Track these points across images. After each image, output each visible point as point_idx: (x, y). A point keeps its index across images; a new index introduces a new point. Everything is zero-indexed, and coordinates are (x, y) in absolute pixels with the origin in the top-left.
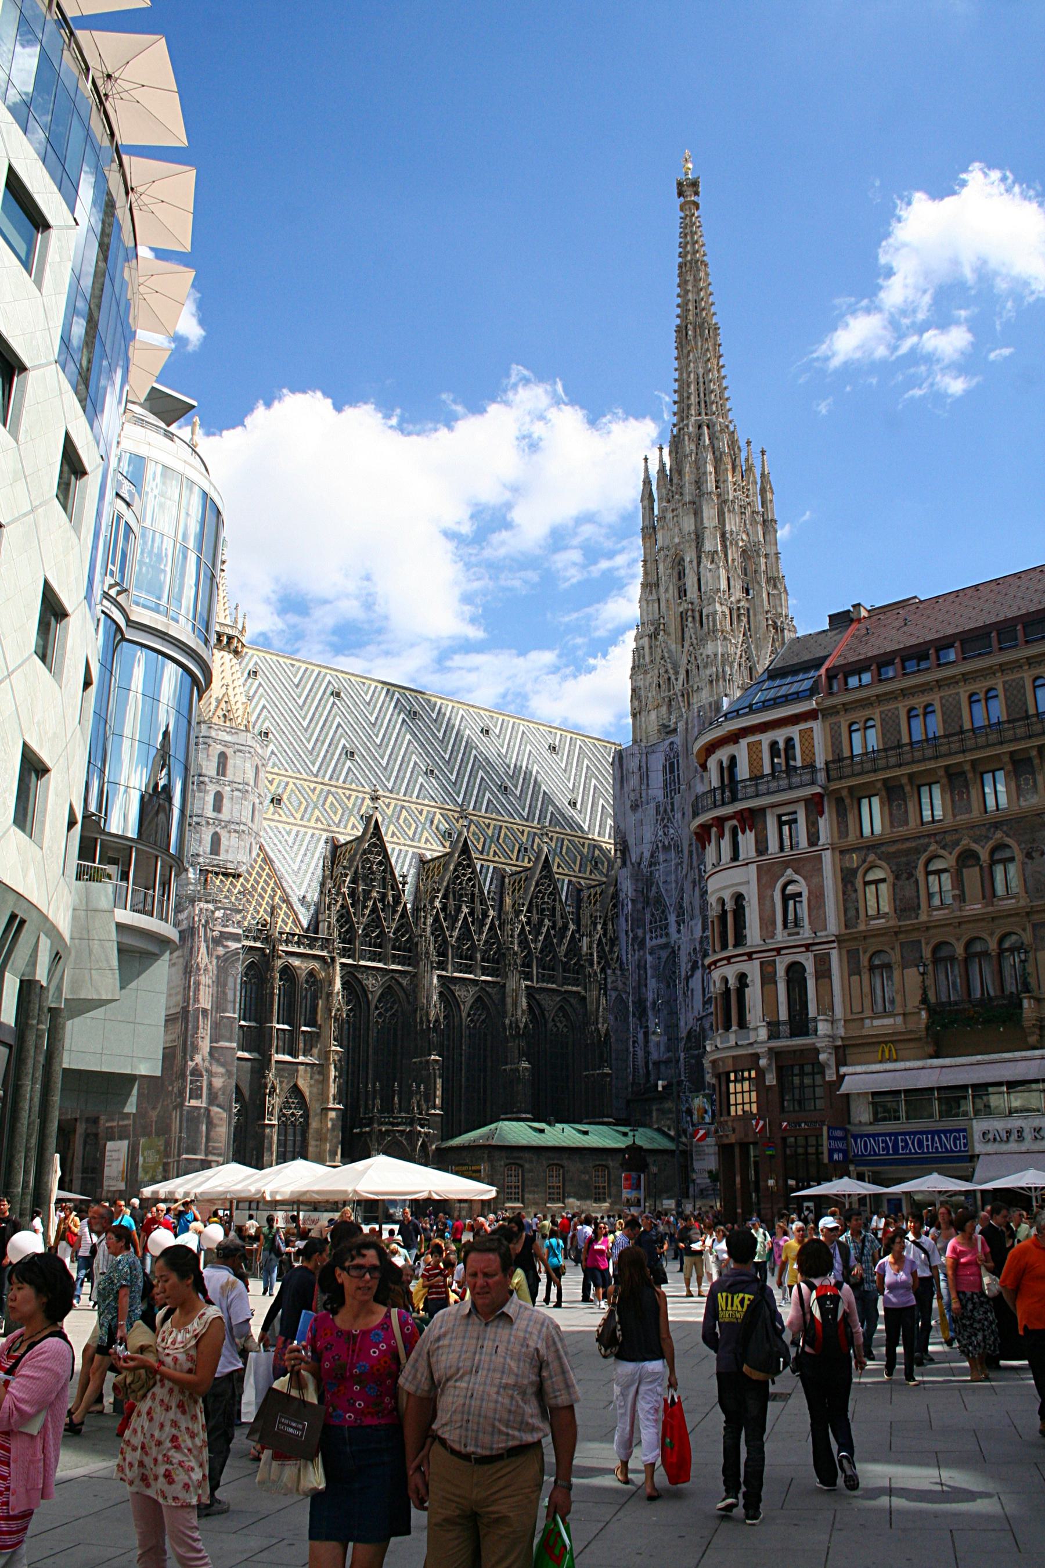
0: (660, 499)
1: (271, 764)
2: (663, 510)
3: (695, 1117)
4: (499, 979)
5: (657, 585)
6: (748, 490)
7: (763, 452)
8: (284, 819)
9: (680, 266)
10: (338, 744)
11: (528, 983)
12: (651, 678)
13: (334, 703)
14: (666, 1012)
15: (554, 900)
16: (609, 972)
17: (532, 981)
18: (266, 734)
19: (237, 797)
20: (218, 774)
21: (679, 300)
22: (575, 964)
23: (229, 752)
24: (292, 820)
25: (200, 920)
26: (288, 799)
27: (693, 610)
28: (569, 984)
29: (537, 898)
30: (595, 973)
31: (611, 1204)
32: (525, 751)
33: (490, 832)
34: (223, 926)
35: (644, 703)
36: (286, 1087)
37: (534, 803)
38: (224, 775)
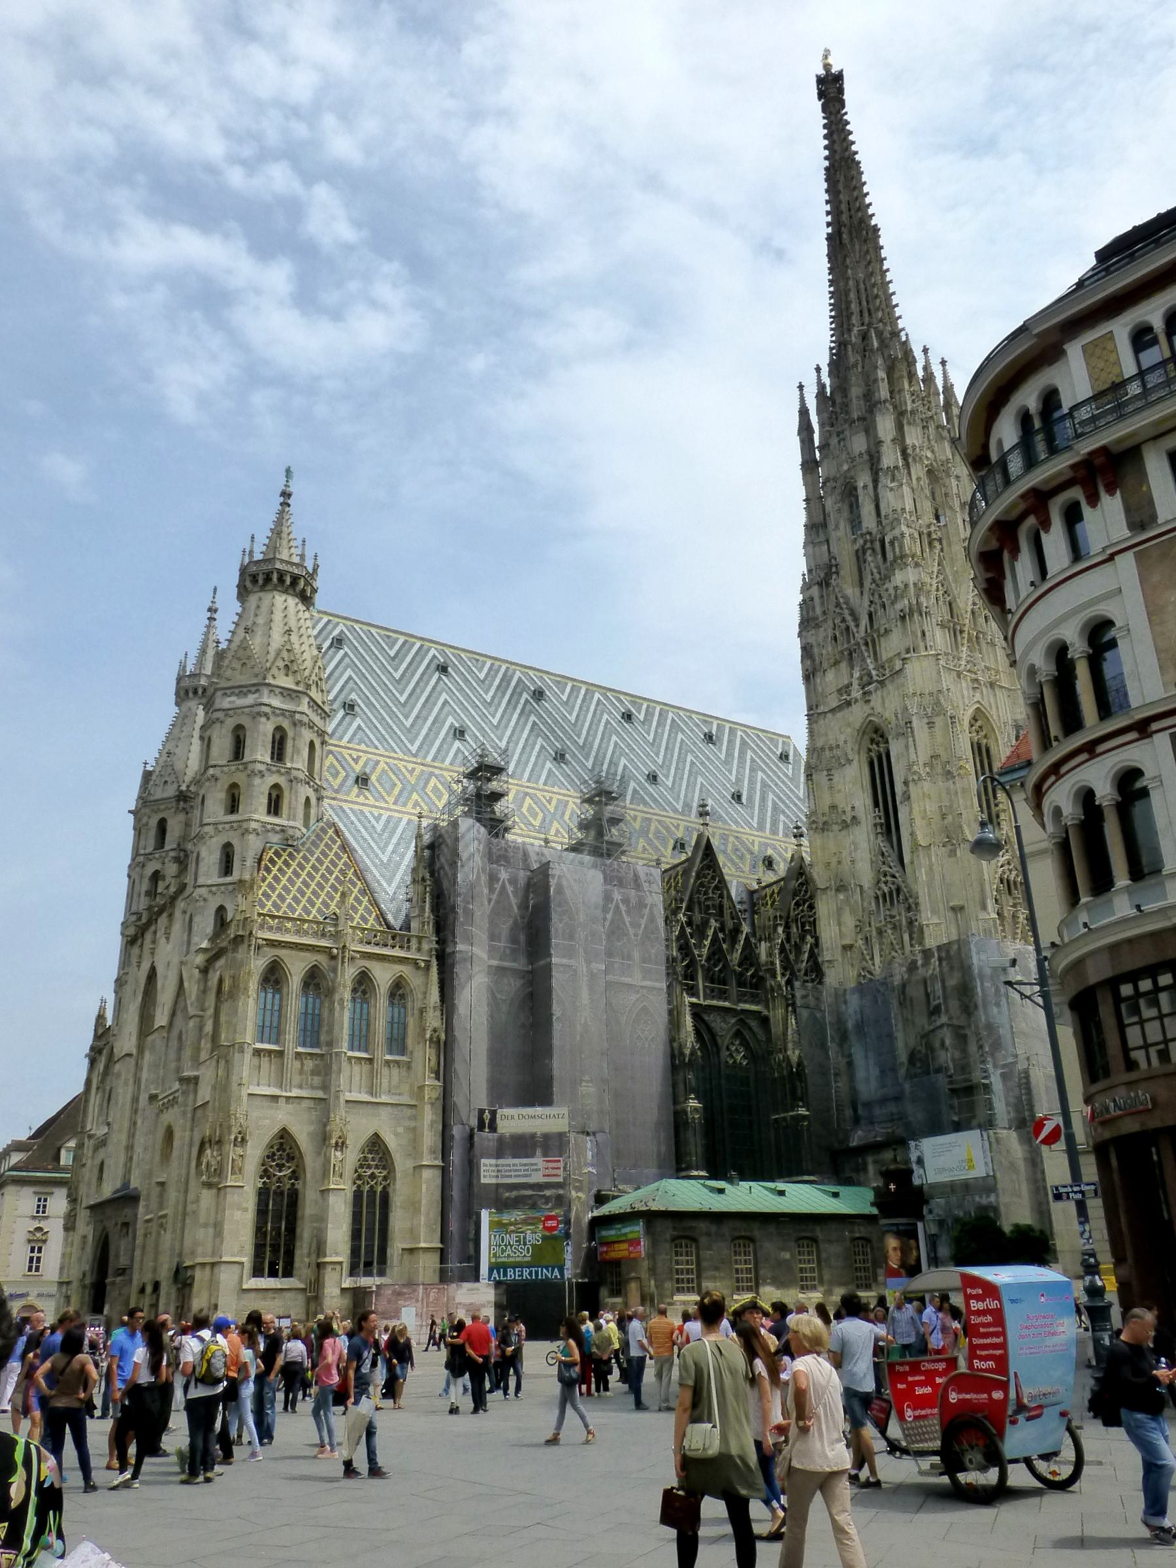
0: (822, 425)
2: (824, 436)
5: (824, 525)
6: (930, 402)
7: (943, 363)
8: (372, 801)
9: (827, 169)
10: (444, 722)
11: (694, 1000)
12: (826, 631)
15: (721, 896)
16: (797, 984)
17: (698, 998)
18: (352, 707)
21: (828, 208)
22: (752, 976)
24: (383, 805)
26: (378, 780)
27: (872, 542)
28: (745, 1002)
29: (699, 892)
30: (780, 986)
33: (637, 825)
35: (817, 662)
37: (690, 795)
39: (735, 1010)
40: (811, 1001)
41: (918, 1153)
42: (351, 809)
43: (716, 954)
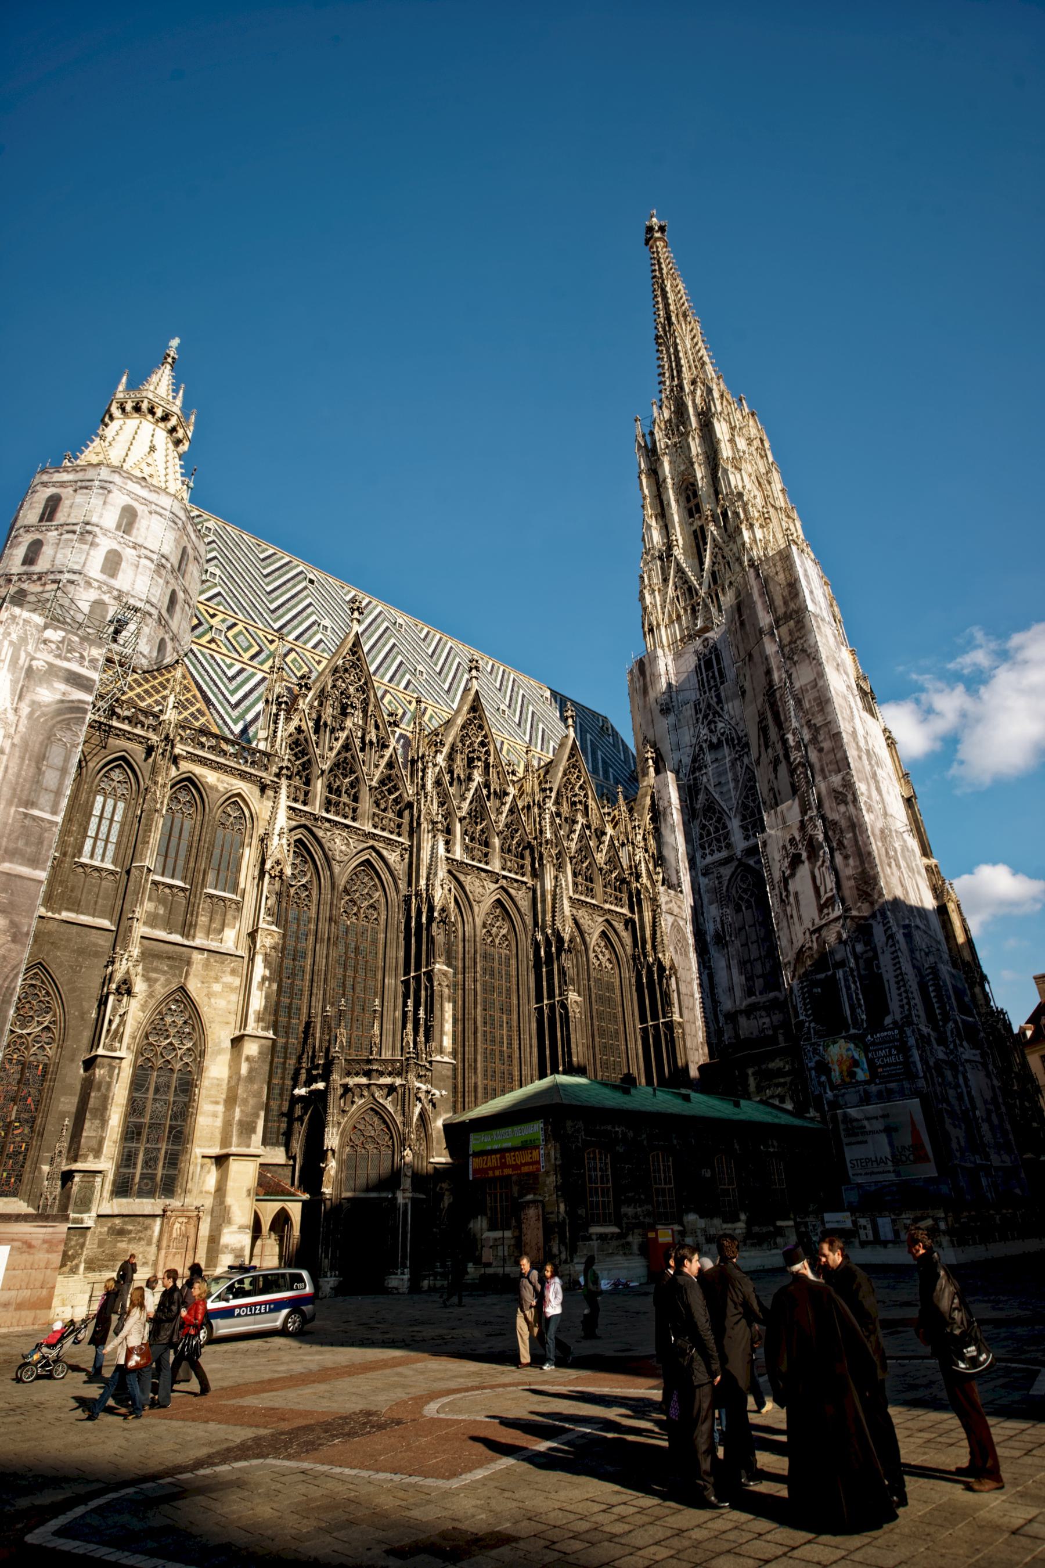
1: (215, 601)
3: (836, 1075)
4: (524, 879)
8: (224, 651)
13: (306, 588)
14: (738, 943)
15: (586, 796)
19: (145, 566)
20: (118, 528)
23: (139, 508)
24: (237, 656)
25: (9, 634)
26: (235, 637)
28: (611, 903)
31: (749, 1223)
32: (518, 693)
34: (59, 656)
36: (161, 990)
38: (127, 531)
39: (602, 908)
40: (673, 905)
41: (817, 1058)
42: (200, 651)
43: (584, 851)
